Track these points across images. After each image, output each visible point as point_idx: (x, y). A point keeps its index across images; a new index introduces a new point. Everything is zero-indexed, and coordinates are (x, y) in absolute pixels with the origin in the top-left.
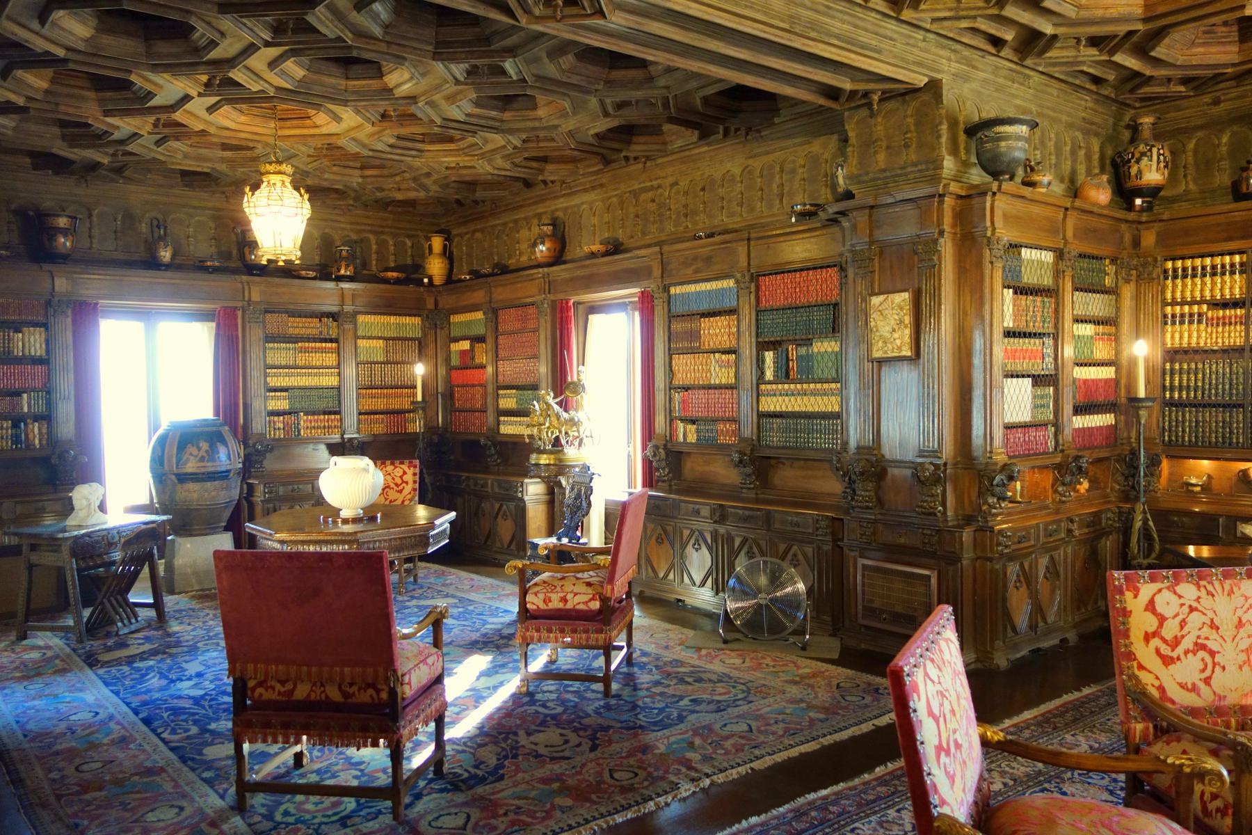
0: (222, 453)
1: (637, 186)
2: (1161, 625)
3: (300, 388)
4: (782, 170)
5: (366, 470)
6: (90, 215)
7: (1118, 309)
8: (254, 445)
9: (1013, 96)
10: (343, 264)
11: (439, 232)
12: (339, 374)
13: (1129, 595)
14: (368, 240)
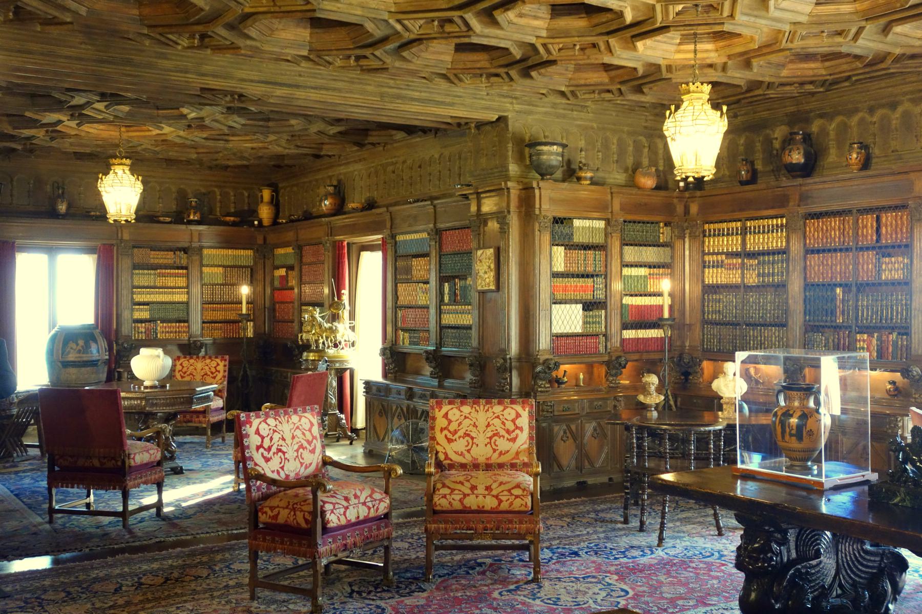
0: (94, 348)
1: (384, 162)
2: (449, 424)
3: (162, 303)
4: (460, 158)
5: (159, 356)
6: (12, 180)
7: (672, 257)
8: (123, 344)
9: (574, 119)
10: (192, 211)
11: (269, 186)
12: (188, 293)
13: (437, 410)
14: (214, 192)
